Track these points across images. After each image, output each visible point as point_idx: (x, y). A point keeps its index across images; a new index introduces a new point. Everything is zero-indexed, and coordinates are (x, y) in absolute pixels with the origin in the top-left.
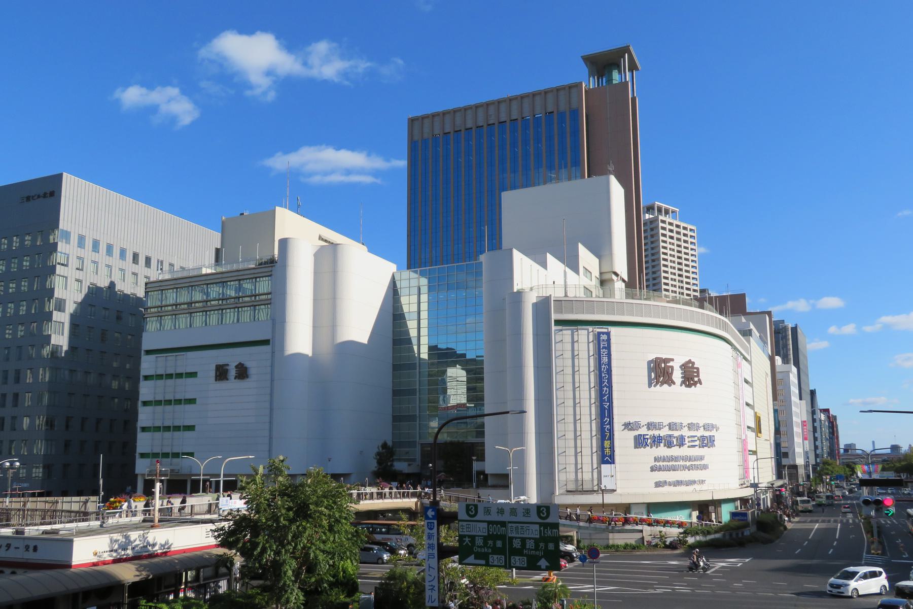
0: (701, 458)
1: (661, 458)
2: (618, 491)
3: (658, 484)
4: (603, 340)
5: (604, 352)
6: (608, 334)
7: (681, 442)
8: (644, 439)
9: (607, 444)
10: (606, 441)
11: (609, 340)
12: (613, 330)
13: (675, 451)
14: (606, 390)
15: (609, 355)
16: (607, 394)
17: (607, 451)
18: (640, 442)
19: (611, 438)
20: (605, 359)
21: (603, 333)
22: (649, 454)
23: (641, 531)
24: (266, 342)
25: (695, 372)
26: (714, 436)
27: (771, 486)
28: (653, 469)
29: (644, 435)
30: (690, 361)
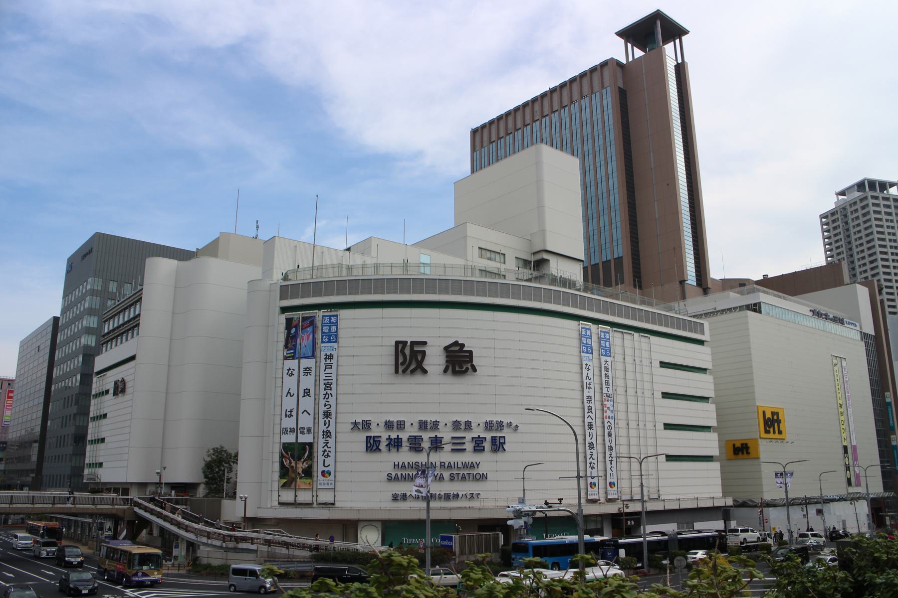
0: (472, 466)
1: (398, 465)
2: (338, 505)
3: (395, 498)
7: (436, 444)
8: (374, 441)
12: (343, 313)
18: (373, 445)
22: (387, 460)
23: (256, 551)
24: (133, 358)
25: (466, 356)
26: (504, 437)
27: (558, 502)
28: (390, 479)
29: (374, 437)
30: (456, 343)
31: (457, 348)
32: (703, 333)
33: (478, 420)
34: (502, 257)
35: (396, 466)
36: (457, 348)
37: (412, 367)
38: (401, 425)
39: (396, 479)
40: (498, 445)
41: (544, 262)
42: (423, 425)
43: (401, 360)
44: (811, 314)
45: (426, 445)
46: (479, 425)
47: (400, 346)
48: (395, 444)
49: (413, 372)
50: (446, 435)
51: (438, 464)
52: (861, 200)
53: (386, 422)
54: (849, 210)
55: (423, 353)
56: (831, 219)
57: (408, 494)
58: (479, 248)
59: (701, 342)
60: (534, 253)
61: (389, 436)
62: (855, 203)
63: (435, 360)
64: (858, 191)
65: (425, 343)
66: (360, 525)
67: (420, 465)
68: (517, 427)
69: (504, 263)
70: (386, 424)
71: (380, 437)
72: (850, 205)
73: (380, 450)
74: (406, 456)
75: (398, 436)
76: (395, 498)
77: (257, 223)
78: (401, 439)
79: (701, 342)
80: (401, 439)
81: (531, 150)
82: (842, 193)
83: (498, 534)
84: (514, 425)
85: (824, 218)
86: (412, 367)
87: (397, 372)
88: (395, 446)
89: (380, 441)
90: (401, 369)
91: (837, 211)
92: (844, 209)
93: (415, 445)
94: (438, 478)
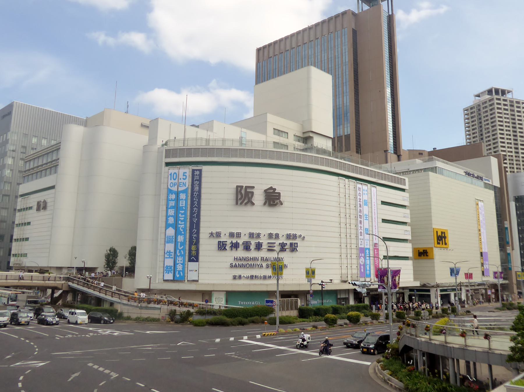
1: (237, 259)
2: (200, 281)
3: (235, 278)
4: (196, 175)
5: (196, 183)
6: (200, 171)
7: (259, 247)
8: (223, 244)
9: (193, 248)
10: (193, 246)
11: (200, 175)
12: (205, 168)
13: (253, 254)
14: (196, 210)
15: (200, 185)
16: (196, 213)
17: (194, 253)
18: (222, 246)
19: (197, 243)
20: (197, 188)
21: (197, 170)
22: (230, 256)
23: (160, 309)
24: (53, 187)
26: (297, 243)
27: (330, 281)
28: (232, 266)
30: (271, 188)
31: (272, 191)
32: (405, 185)
33: (283, 233)
34: (286, 134)
35: (236, 259)
36: (272, 191)
37: (246, 201)
38: (239, 235)
39: (236, 266)
40: (294, 248)
41: (310, 138)
42: (251, 235)
43: (239, 197)
44: (464, 174)
45: (253, 247)
46: (283, 236)
47: (239, 188)
48: (235, 246)
49: (246, 204)
50: (264, 241)
51: (260, 259)
52: (490, 101)
53: (230, 233)
54: (482, 106)
55: (252, 193)
56: (470, 111)
57: (242, 276)
58: (274, 129)
59: (403, 190)
60: (304, 133)
61: (232, 241)
62: (486, 102)
63: (259, 198)
64: (488, 95)
65: (253, 187)
66: (213, 292)
67: (249, 258)
68: (304, 237)
69: (287, 138)
70: (230, 234)
71: (227, 241)
72: (483, 104)
73: (226, 249)
74: (241, 253)
75: (237, 241)
76: (235, 278)
77: (128, 103)
78: (239, 243)
79: (403, 190)
80: (239, 243)
81: (305, 69)
82: (478, 96)
83: (297, 299)
84: (302, 236)
85: (466, 110)
86: (246, 201)
87: (237, 204)
88: (235, 247)
89: (226, 244)
90: (239, 202)
91: (474, 107)
92: (479, 105)
93: (247, 247)
94: (259, 266)
